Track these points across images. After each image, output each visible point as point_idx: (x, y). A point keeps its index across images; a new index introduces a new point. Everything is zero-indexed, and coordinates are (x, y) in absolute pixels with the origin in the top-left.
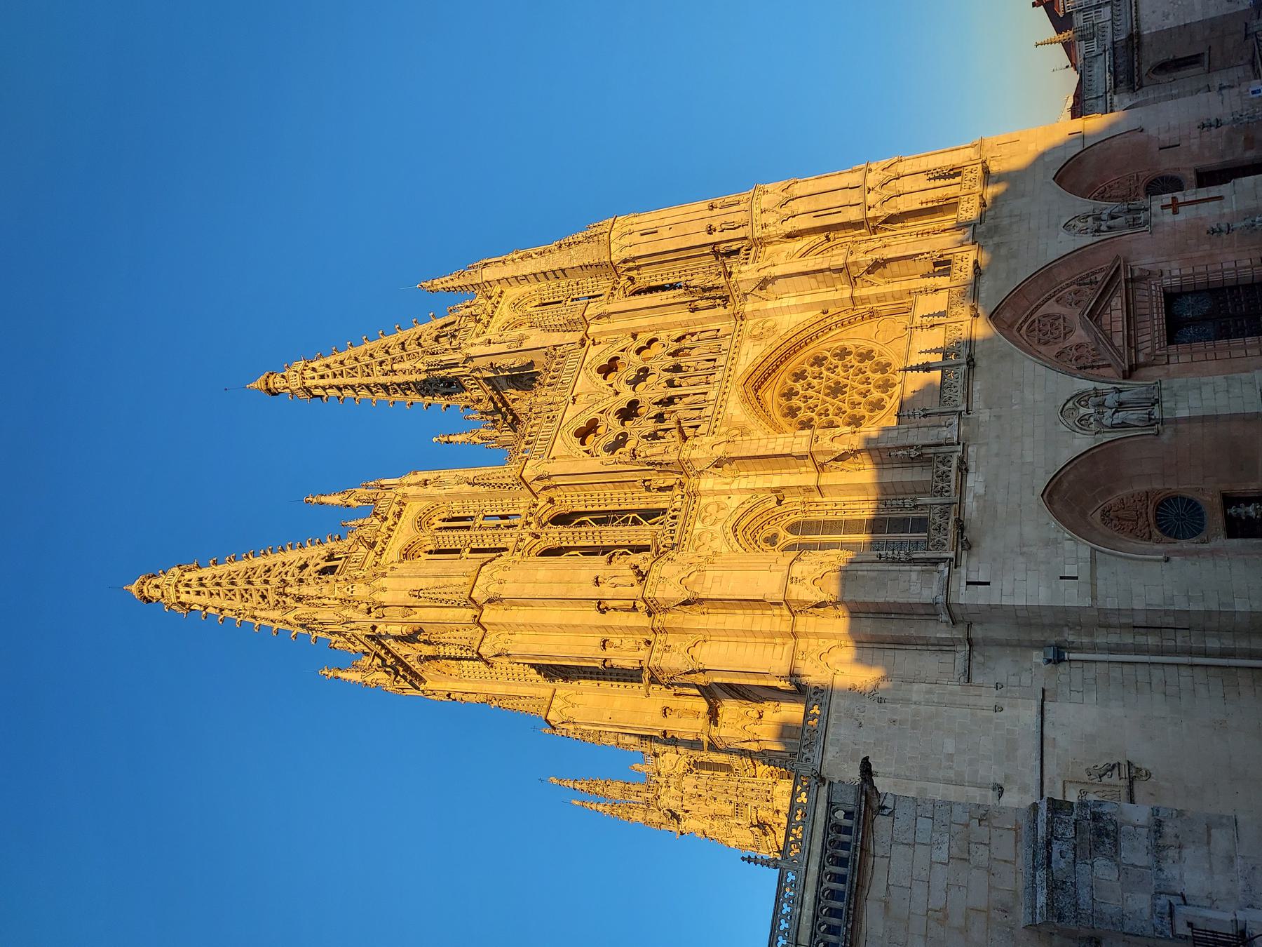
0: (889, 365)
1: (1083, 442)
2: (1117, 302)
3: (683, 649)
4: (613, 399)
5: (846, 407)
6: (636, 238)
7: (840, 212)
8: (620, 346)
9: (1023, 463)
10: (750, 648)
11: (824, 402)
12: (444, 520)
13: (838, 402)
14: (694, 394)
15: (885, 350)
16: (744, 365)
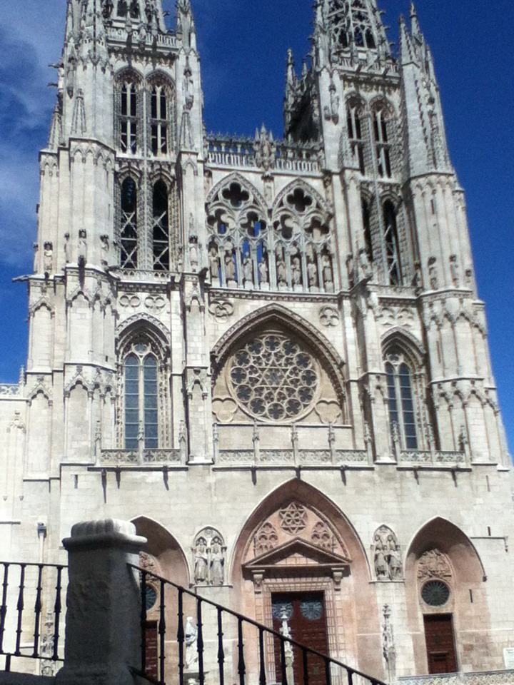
0: (296, 412)
1: (185, 540)
2: (312, 563)
3: (43, 300)
4: (266, 209)
5: (258, 385)
6: (429, 197)
7: (440, 361)
8: (322, 204)
9: (170, 505)
10: (46, 344)
11: (263, 370)
12: (162, 93)
13: (261, 380)
14: (268, 273)
15: (309, 409)
16: (294, 307)
